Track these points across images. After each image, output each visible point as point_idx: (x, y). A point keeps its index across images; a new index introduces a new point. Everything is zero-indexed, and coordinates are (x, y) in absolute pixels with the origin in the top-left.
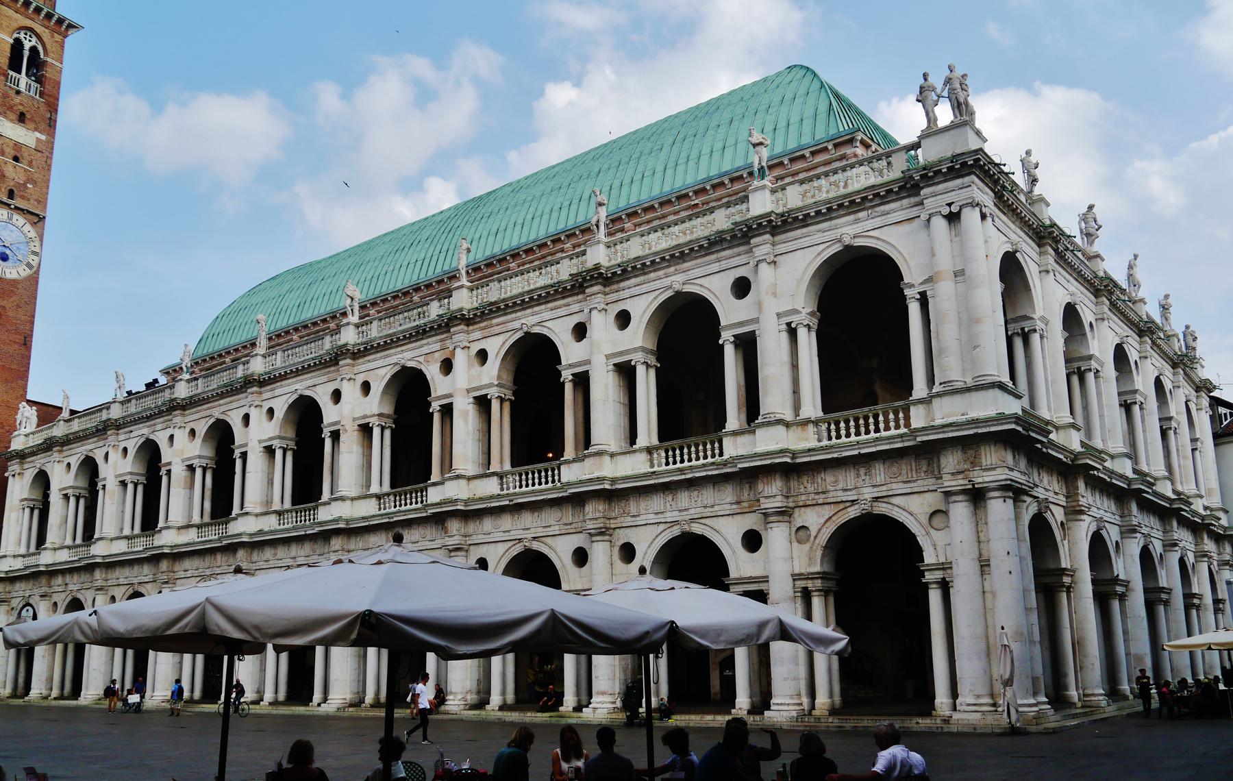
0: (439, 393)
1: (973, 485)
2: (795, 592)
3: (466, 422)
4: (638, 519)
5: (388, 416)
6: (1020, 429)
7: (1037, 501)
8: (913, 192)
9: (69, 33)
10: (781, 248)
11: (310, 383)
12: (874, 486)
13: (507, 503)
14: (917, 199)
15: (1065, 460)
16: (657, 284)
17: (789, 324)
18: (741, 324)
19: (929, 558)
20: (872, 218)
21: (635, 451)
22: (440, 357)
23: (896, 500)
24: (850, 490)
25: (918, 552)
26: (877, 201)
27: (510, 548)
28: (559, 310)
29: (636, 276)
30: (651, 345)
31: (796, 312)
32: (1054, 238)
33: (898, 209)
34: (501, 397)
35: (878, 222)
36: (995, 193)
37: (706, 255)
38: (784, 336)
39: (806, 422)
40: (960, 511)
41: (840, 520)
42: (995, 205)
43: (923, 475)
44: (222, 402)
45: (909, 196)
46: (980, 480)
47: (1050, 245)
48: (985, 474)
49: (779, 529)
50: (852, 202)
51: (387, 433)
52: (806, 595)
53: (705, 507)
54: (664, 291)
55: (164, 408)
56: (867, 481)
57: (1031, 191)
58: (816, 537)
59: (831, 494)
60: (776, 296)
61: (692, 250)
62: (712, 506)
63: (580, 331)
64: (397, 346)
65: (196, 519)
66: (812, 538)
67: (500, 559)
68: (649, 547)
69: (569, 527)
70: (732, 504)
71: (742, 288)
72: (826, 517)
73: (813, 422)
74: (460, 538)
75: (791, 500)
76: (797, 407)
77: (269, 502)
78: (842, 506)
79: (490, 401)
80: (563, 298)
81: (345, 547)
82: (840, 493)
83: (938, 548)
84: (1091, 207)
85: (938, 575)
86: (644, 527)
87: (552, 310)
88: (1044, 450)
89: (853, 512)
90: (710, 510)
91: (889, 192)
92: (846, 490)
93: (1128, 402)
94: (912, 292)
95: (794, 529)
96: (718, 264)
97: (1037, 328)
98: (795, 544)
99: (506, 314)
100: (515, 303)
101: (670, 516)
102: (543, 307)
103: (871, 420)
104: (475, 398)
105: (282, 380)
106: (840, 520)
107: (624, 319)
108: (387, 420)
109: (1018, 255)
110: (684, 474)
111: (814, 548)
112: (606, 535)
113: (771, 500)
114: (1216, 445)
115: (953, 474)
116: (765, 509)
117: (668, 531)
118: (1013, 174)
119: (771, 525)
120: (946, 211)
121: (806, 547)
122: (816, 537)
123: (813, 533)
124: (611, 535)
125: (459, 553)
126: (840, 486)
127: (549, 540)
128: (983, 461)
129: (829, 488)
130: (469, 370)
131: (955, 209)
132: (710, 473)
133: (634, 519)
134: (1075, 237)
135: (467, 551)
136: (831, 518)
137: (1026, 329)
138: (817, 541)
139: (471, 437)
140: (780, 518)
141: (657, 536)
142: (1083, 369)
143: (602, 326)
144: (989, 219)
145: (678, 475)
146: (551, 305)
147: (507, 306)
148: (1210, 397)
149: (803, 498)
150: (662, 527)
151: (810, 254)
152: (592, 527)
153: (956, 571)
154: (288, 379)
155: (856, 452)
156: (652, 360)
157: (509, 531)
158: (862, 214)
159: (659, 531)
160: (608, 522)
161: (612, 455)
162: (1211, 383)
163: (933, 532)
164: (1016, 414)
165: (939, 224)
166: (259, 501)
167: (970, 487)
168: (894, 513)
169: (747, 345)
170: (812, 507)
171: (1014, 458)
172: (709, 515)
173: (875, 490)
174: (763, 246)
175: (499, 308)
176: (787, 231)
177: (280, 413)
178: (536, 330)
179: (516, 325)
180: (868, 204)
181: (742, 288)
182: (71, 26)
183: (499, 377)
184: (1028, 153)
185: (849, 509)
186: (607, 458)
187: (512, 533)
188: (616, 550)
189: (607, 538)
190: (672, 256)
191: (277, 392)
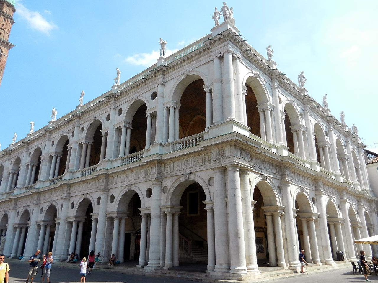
0: (70, 143)
1: (222, 165)
2: (161, 214)
3: (75, 153)
4: (116, 185)
5: (59, 153)
6: (241, 140)
7: (262, 176)
8: (209, 51)
9: (11, 47)
10: (167, 80)
11: (40, 143)
12: (189, 168)
13: (79, 181)
14: (210, 54)
15: (277, 159)
16: (130, 98)
17: (167, 107)
18: (153, 108)
19: (207, 197)
20: (195, 64)
21: (118, 159)
22: (72, 131)
23: (198, 174)
24: (181, 170)
25: (203, 197)
26: (197, 57)
27: (81, 197)
29: (125, 96)
30: (130, 120)
31: (169, 102)
32: (277, 76)
33: (204, 59)
34: (87, 143)
35: (197, 65)
36: (244, 52)
37: (145, 85)
38: (165, 111)
39: (168, 145)
40: (217, 177)
41: (178, 183)
42: (242, 55)
43: (206, 162)
44: (19, 151)
45: (208, 53)
46: (225, 163)
47: (276, 79)
48: (227, 160)
49: (156, 187)
50: (188, 59)
51: (59, 159)
52: (165, 215)
53: (136, 180)
54: (132, 101)
55: (5, 154)
56: (187, 166)
57: (269, 60)
58: (169, 190)
59: (175, 172)
60: (164, 97)
61: (140, 84)
62: (138, 179)
63: (108, 118)
64: (62, 128)
65: (8, 191)
66: (168, 191)
67: (77, 203)
68: (118, 196)
69: (97, 189)
70: (144, 178)
71: (154, 96)
72: (173, 182)
73: (172, 144)
74: (67, 194)
75: (162, 175)
76: (167, 138)
78: (178, 177)
79: (83, 144)
80: (105, 106)
81: (39, 199)
82: (178, 172)
83: (211, 194)
84: (302, 73)
85: (211, 205)
86: (118, 188)
87: (102, 111)
88: (263, 153)
89: (182, 179)
90: (137, 180)
91: (200, 52)
92: (180, 170)
93: (323, 146)
94: (207, 90)
95: (162, 187)
96: (148, 88)
97: (268, 109)
98: (162, 193)
99: (90, 114)
100: (91, 110)
101: (126, 183)
102: (100, 110)
103: (191, 142)
104: (79, 144)
105: (34, 142)
106: (178, 183)
107: (120, 112)
108: (58, 154)
109: (258, 79)
110: (128, 166)
111: (168, 195)
112: (106, 191)
113: (154, 175)
114: (367, 167)
115: (215, 161)
116: (151, 179)
117: (125, 189)
118: (241, 35)
119: (154, 185)
120: (219, 55)
121: (166, 194)
122: (169, 190)
123: (168, 189)
124: (108, 192)
125: (66, 200)
126: (178, 168)
127: (91, 194)
128: (226, 154)
129: (175, 169)
130: (79, 134)
131: (221, 55)
132: (136, 166)
133: (115, 185)
134: (285, 74)
135: (69, 199)
136: (174, 182)
137: (264, 109)
138: (169, 192)
139: (76, 158)
140: (156, 182)
141: (121, 192)
142: (297, 130)
143: (113, 114)
144: (238, 61)
145: (126, 167)
146: (101, 110)
147: (89, 111)
148: (364, 150)
149: (166, 174)
150: (123, 188)
151: (175, 80)
152: (101, 188)
153: (215, 204)
154: (35, 142)
155: (181, 154)
156: (130, 126)
157: (81, 191)
158: (192, 63)
159: (122, 189)
160: (107, 186)
161: (111, 161)
162: (363, 144)
163: (209, 186)
164: (236, 132)
165: (216, 61)
166: (22, 184)
167: (220, 166)
168: (196, 179)
169: (154, 116)
170: (169, 178)
171: (241, 153)
172: (137, 182)
173: (190, 170)
174: (160, 79)
175: (87, 112)
176: (169, 73)
177: (32, 154)
178: (97, 119)
179: (92, 118)
180: (194, 58)
181: (154, 96)
182: (10, 45)
183: (86, 136)
184: (269, 47)
185: (181, 178)
186: (109, 163)
187: (82, 192)
188: (109, 197)
189: (106, 192)
190: (134, 87)
191: (33, 146)
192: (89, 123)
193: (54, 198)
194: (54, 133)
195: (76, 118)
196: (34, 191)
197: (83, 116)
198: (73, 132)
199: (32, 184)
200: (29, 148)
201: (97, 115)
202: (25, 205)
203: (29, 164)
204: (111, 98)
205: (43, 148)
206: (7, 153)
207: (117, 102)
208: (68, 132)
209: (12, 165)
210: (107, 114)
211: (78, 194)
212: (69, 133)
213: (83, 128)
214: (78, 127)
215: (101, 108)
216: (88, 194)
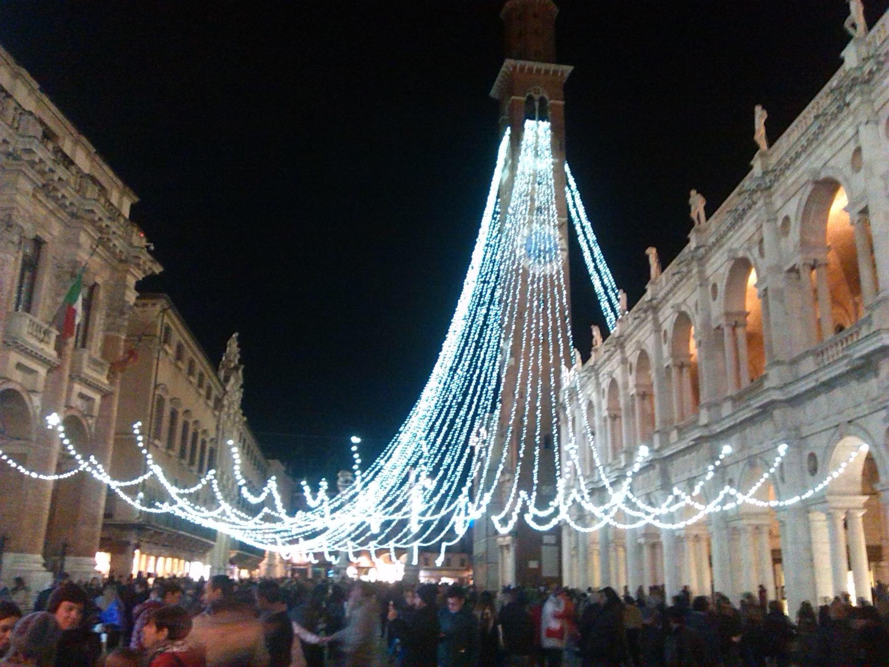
11: (681, 300)
13: (813, 384)
22: (756, 238)
28: (837, 143)
44: (641, 334)
77: (671, 421)
80: (838, 126)
87: (831, 145)
102: (823, 146)
146: (829, 142)
177: (670, 334)
178: (823, 175)
179: (805, 178)
192: (800, 200)
193: (755, 450)
194: (711, 261)
195: (759, 194)
196: (697, 434)
197: (776, 185)
198: (761, 241)
199: (690, 417)
200: (661, 319)
201: (818, 164)
202: (687, 475)
203: (670, 362)
204: (850, 89)
205: (694, 310)
206: (615, 346)
207: (873, 95)
208: (746, 245)
209: (634, 372)
210: (852, 147)
211: (820, 425)
212: (749, 249)
213: (787, 219)
214: (768, 221)
215: (825, 139)
216: (850, 422)
